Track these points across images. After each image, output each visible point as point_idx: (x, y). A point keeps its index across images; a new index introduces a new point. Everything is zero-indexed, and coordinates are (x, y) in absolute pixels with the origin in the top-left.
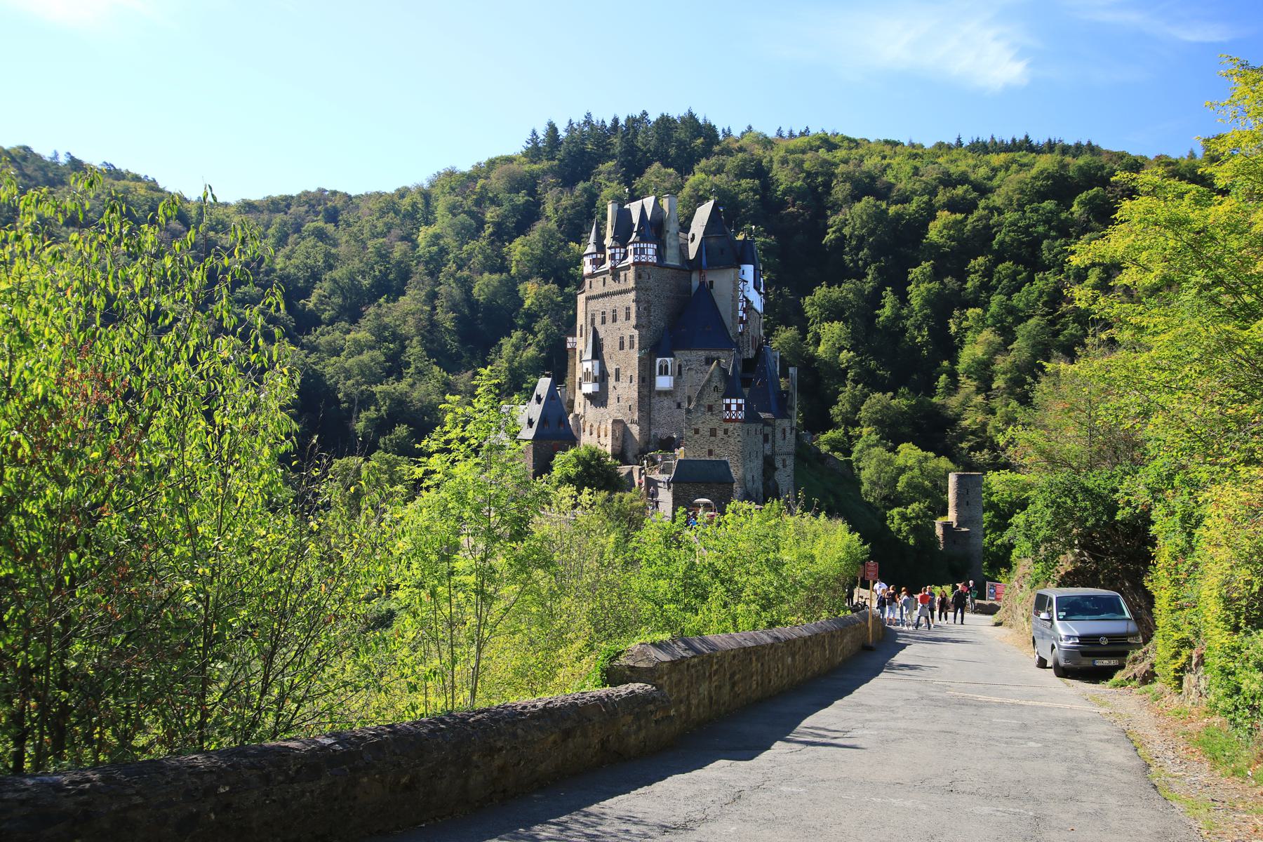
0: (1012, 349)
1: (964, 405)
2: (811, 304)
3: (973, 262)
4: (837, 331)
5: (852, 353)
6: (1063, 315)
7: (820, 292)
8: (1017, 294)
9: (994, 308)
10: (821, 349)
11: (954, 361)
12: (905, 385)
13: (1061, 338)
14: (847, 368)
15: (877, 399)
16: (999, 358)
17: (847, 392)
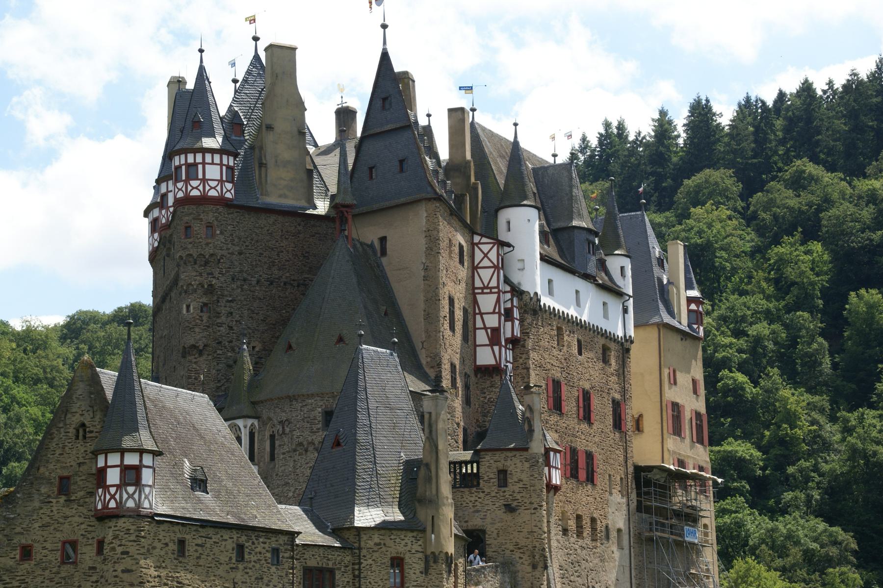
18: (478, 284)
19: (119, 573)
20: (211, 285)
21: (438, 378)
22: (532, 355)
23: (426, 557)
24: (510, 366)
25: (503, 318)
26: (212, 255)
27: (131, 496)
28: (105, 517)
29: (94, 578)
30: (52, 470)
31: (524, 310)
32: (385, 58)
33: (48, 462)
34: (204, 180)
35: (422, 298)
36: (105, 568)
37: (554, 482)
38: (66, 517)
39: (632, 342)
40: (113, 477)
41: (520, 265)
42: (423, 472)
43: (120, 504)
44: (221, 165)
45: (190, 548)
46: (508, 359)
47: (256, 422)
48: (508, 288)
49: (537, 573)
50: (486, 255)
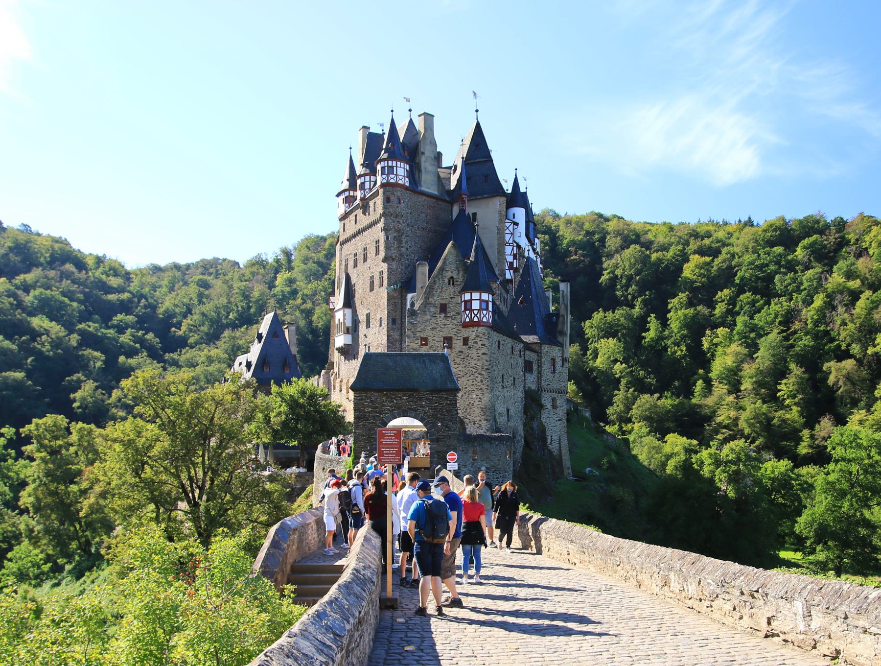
0: (757, 357)
1: (718, 404)
2: (590, 327)
3: (719, 293)
4: (612, 346)
5: (624, 365)
6: (795, 332)
7: (598, 316)
8: (758, 315)
9: (739, 327)
10: (599, 360)
11: (708, 370)
12: (668, 390)
13: (797, 349)
14: (620, 377)
15: (645, 400)
16: (746, 366)
17: (619, 397)
19: (480, 354)
23: (563, 359)
27: (485, 316)
28: (466, 325)
29: (462, 356)
30: (436, 300)
33: (433, 295)
35: (496, 242)
36: (470, 352)
38: (445, 325)
40: (476, 305)
41: (519, 235)
42: (561, 319)
43: (480, 321)
45: (501, 346)
48: (515, 244)
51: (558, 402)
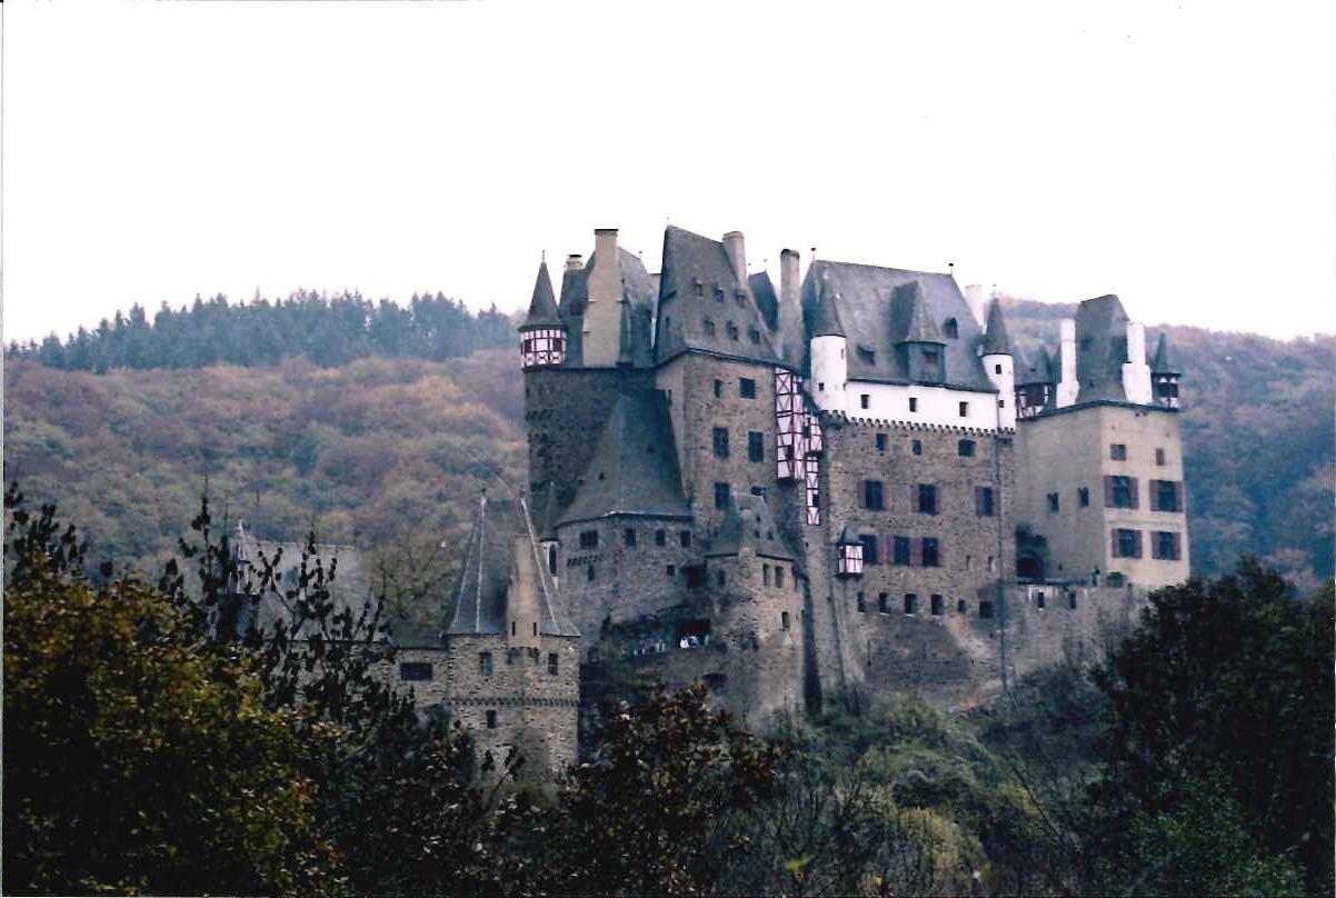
18: (779, 409)
20: (544, 435)
21: (691, 500)
22: (833, 464)
24: (813, 477)
25: (799, 437)
26: (545, 411)
31: (823, 427)
32: (666, 233)
34: (536, 352)
35: (682, 434)
37: (851, 570)
39: (1014, 433)
44: (549, 338)
46: (809, 469)
47: (556, 543)
49: (746, 652)
50: (783, 384)
51: (500, 718)
